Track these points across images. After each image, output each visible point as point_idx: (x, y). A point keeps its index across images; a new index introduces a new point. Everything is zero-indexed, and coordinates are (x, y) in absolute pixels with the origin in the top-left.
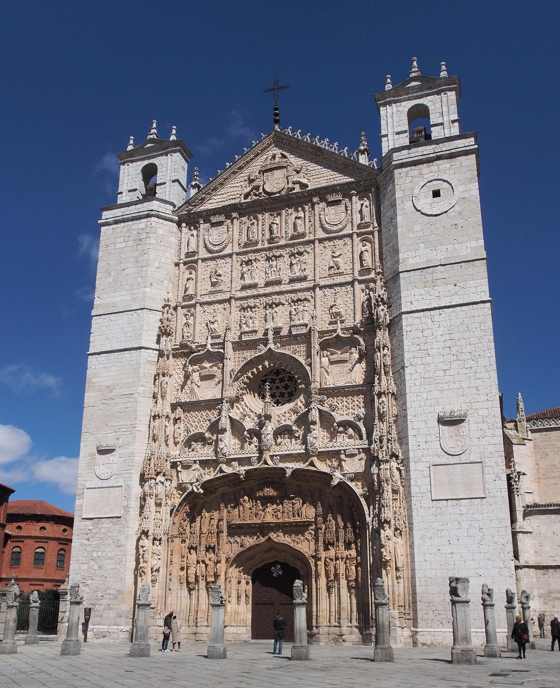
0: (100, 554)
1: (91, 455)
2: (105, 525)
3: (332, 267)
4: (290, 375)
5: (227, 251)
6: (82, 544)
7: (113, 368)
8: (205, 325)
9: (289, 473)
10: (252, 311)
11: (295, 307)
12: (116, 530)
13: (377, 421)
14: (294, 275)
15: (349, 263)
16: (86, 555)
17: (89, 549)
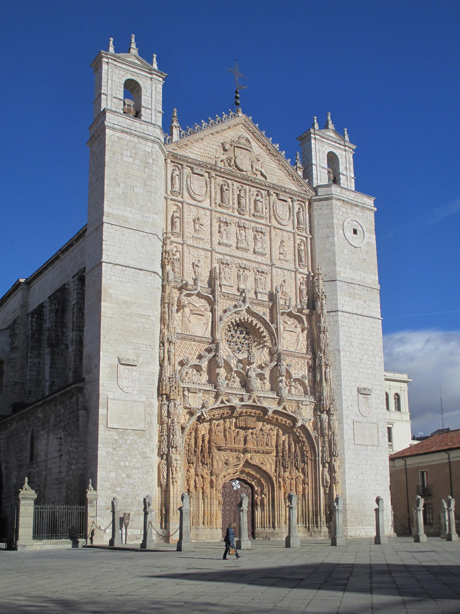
0: (127, 463)
1: (111, 366)
2: (130, 437)
3: (282, 254)
4: (246, 330)
5: (206, 204)
6: (108, 453)
7: (129, 285)
8: (191, 266)
9: (270, 413)
10: (229, 268)
11: (260, 277)
12: (141, 442)
13: (324, 384)
14: (258, 250)
15: (291, 254)
16: (114, 464)
17: (116, 458)
